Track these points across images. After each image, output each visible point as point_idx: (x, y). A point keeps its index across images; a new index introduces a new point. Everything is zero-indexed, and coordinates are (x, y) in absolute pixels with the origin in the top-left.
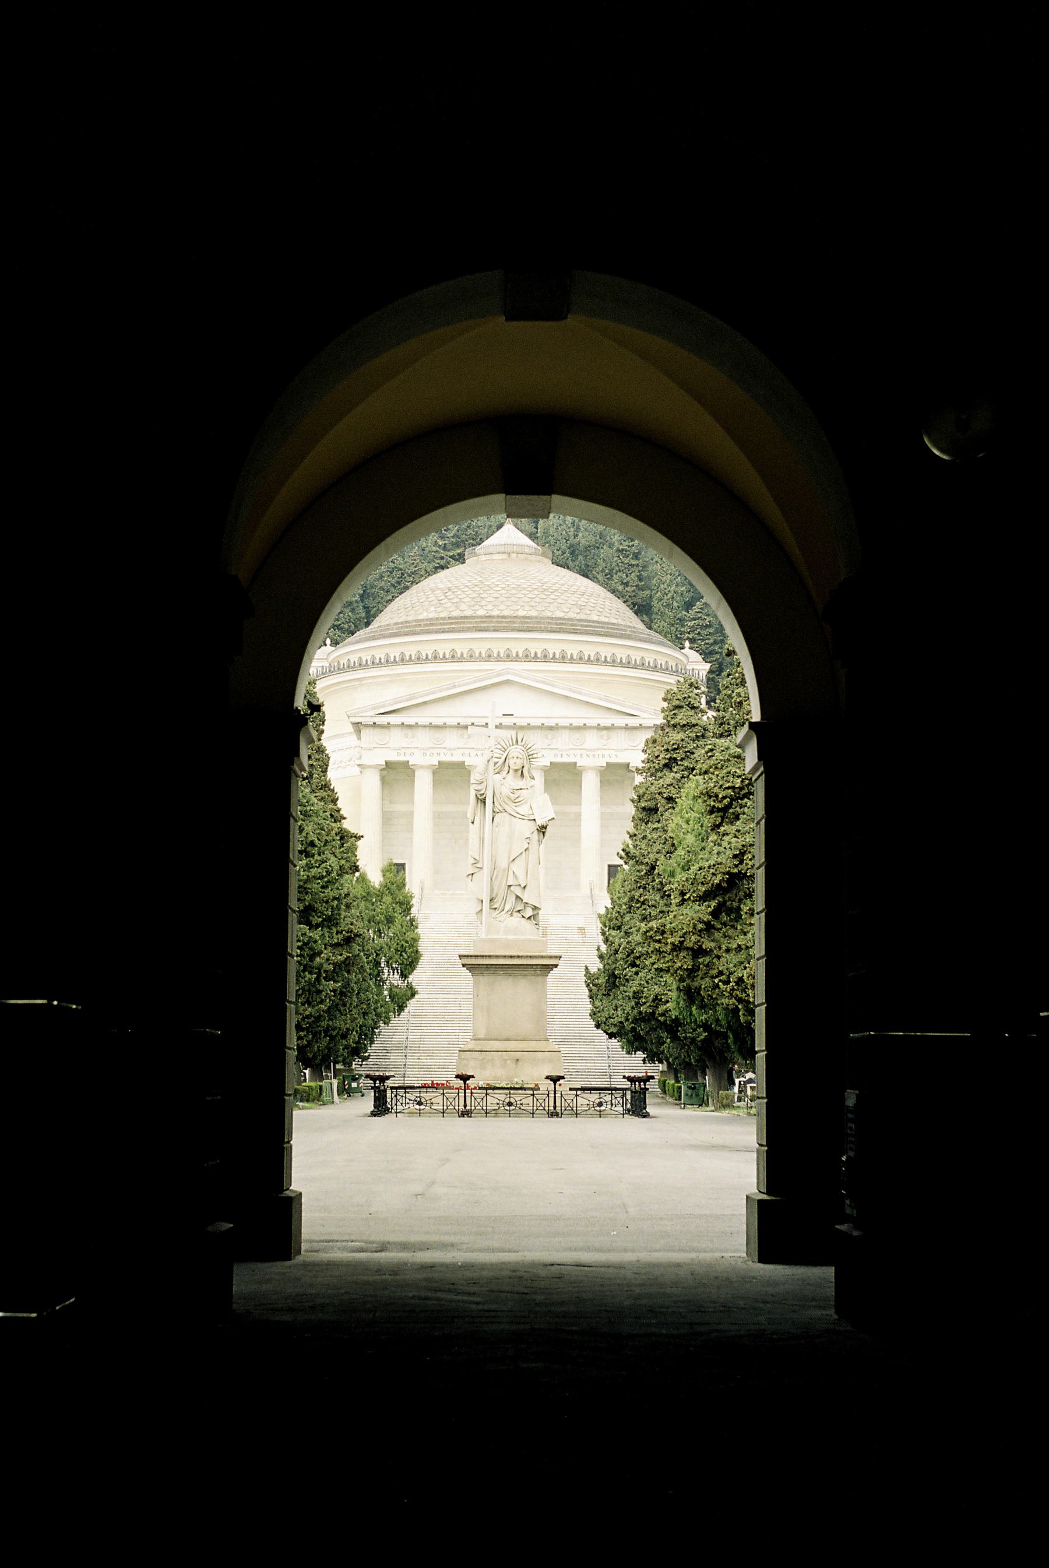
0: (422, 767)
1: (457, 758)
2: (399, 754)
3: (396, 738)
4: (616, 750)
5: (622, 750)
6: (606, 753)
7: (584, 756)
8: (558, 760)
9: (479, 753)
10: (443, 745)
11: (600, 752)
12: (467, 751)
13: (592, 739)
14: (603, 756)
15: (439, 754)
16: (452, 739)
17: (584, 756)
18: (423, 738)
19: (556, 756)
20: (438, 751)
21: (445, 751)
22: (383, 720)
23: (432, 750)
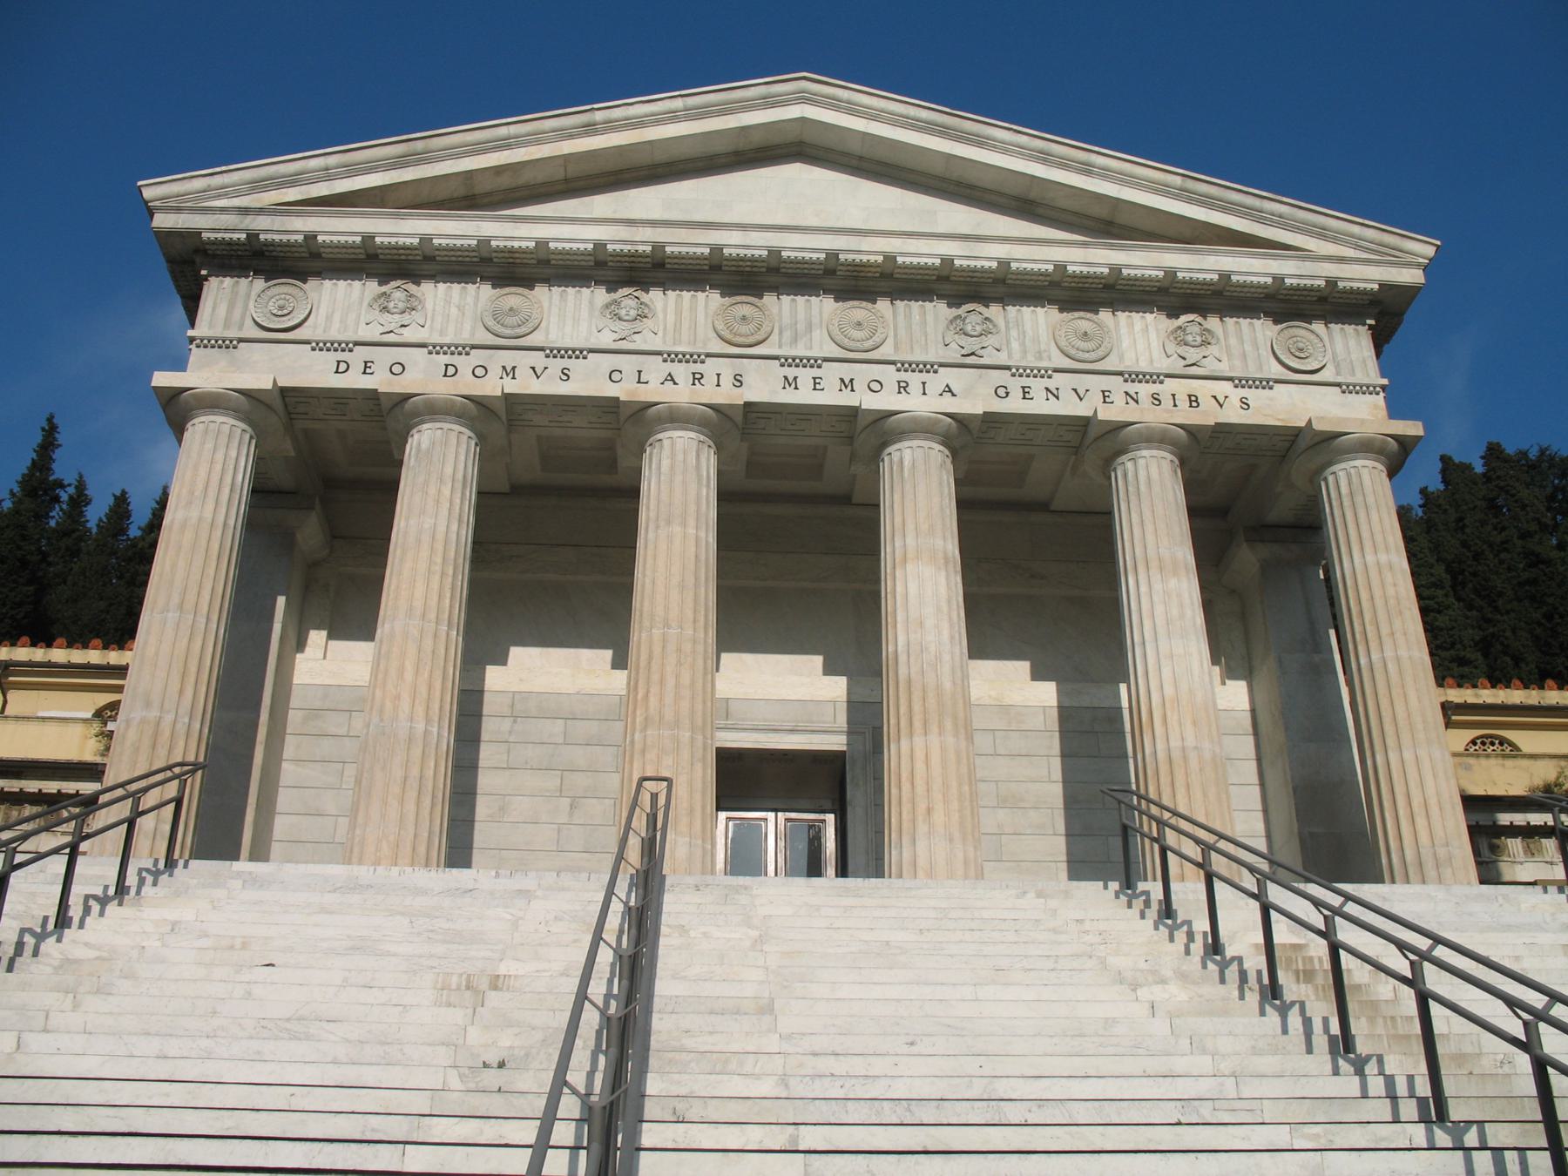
0: (435, 410)
1: (589, 381)
2: (341, 368)
3: (339, 304)
4: (1239, 382)
5: (1267, 384)
6: (1203, 389)
7: (1118, 398)
8: (1014, 405)
9: (682, 371)
10: (536, 339)
11: (1181, 387)
12: (628, 364)
13: (1140, 337)
14: (1193, 400)
15: (510, 372)
16: (569, 314)
17: (1118, 398)
18: (450, 308)
19: (1002, 392)
20: (508, 358)
21: (538, 359)
22: (299, 226)
23: (478, 357)
